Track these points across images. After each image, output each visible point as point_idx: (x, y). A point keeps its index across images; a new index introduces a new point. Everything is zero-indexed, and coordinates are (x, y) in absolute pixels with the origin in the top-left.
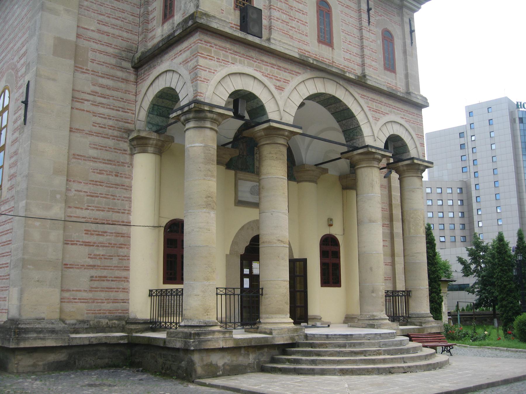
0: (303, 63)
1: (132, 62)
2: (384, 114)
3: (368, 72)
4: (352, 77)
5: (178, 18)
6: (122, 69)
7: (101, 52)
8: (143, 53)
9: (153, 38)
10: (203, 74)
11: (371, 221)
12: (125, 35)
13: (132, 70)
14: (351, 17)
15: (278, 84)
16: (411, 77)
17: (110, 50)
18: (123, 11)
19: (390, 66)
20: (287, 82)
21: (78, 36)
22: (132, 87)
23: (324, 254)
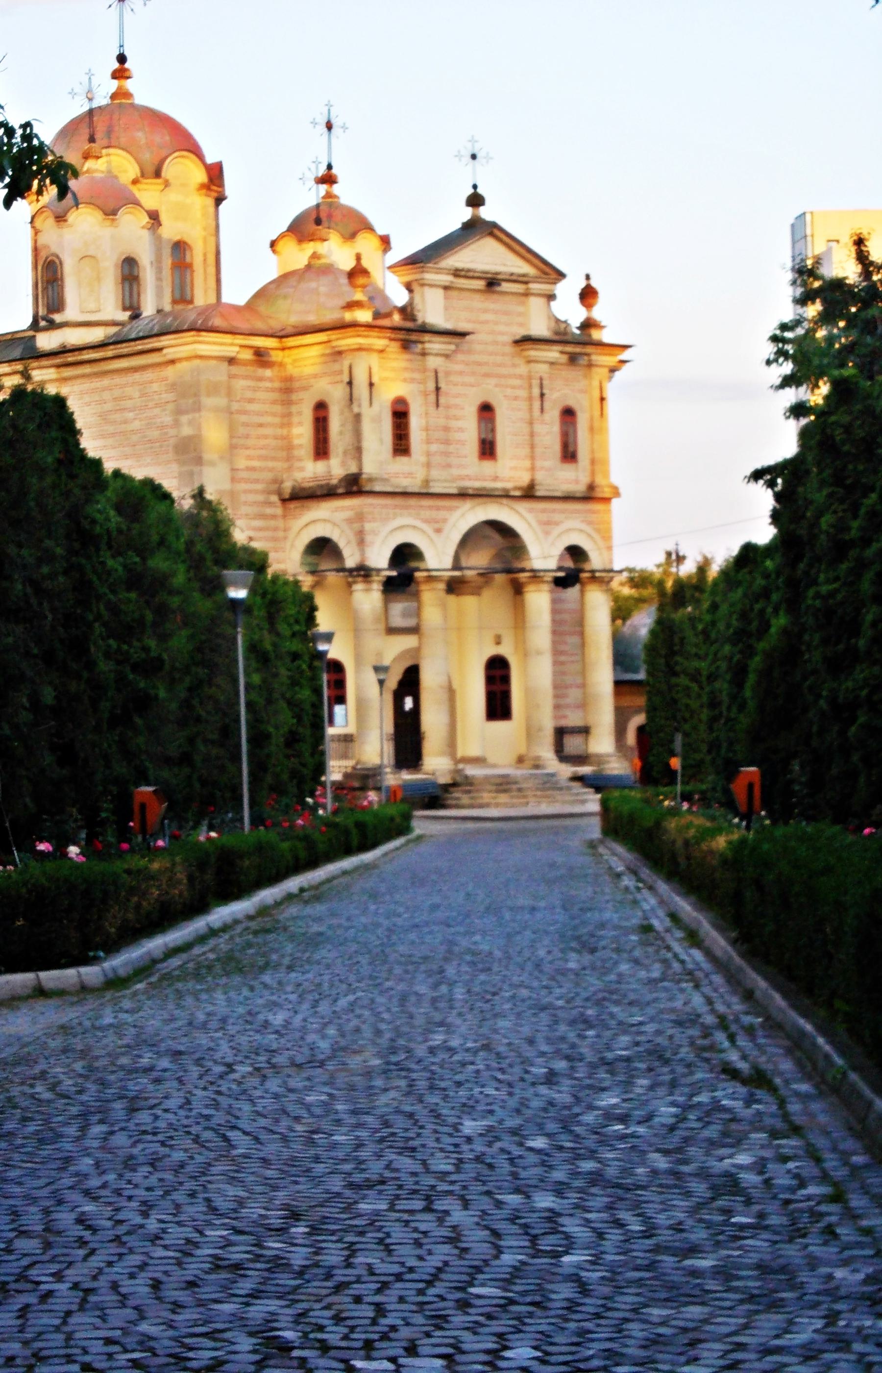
0: (463, 495)
1: (279, 493)
2: (557, 524)
3: (540, 476)
4: (518, 493)
5: (336, 468)
6: (270, 504)
7: (250, 491)
8: (294, 488)
9: (302, 469)
10: (368, 538)
11: (539, 653)
12: (270, 464)
13: (279, 503)
14: (519, 410)
15: (437, 526)
16: (598, 463)
17: (259, 487)
18: (266, 437)
19: (569, 455)
20: (445, 521)
21: (233, 480)
22: (280, 523)
23: (490, 680)
